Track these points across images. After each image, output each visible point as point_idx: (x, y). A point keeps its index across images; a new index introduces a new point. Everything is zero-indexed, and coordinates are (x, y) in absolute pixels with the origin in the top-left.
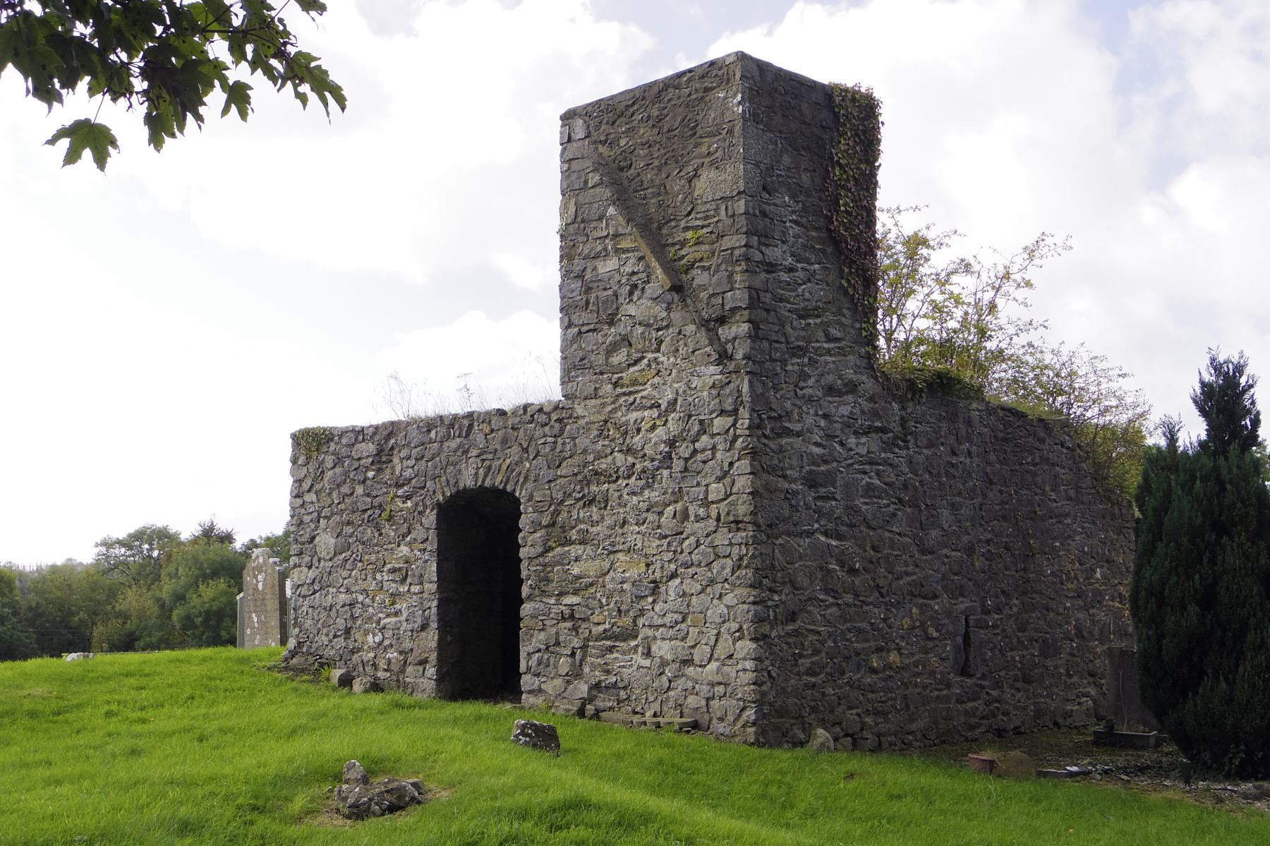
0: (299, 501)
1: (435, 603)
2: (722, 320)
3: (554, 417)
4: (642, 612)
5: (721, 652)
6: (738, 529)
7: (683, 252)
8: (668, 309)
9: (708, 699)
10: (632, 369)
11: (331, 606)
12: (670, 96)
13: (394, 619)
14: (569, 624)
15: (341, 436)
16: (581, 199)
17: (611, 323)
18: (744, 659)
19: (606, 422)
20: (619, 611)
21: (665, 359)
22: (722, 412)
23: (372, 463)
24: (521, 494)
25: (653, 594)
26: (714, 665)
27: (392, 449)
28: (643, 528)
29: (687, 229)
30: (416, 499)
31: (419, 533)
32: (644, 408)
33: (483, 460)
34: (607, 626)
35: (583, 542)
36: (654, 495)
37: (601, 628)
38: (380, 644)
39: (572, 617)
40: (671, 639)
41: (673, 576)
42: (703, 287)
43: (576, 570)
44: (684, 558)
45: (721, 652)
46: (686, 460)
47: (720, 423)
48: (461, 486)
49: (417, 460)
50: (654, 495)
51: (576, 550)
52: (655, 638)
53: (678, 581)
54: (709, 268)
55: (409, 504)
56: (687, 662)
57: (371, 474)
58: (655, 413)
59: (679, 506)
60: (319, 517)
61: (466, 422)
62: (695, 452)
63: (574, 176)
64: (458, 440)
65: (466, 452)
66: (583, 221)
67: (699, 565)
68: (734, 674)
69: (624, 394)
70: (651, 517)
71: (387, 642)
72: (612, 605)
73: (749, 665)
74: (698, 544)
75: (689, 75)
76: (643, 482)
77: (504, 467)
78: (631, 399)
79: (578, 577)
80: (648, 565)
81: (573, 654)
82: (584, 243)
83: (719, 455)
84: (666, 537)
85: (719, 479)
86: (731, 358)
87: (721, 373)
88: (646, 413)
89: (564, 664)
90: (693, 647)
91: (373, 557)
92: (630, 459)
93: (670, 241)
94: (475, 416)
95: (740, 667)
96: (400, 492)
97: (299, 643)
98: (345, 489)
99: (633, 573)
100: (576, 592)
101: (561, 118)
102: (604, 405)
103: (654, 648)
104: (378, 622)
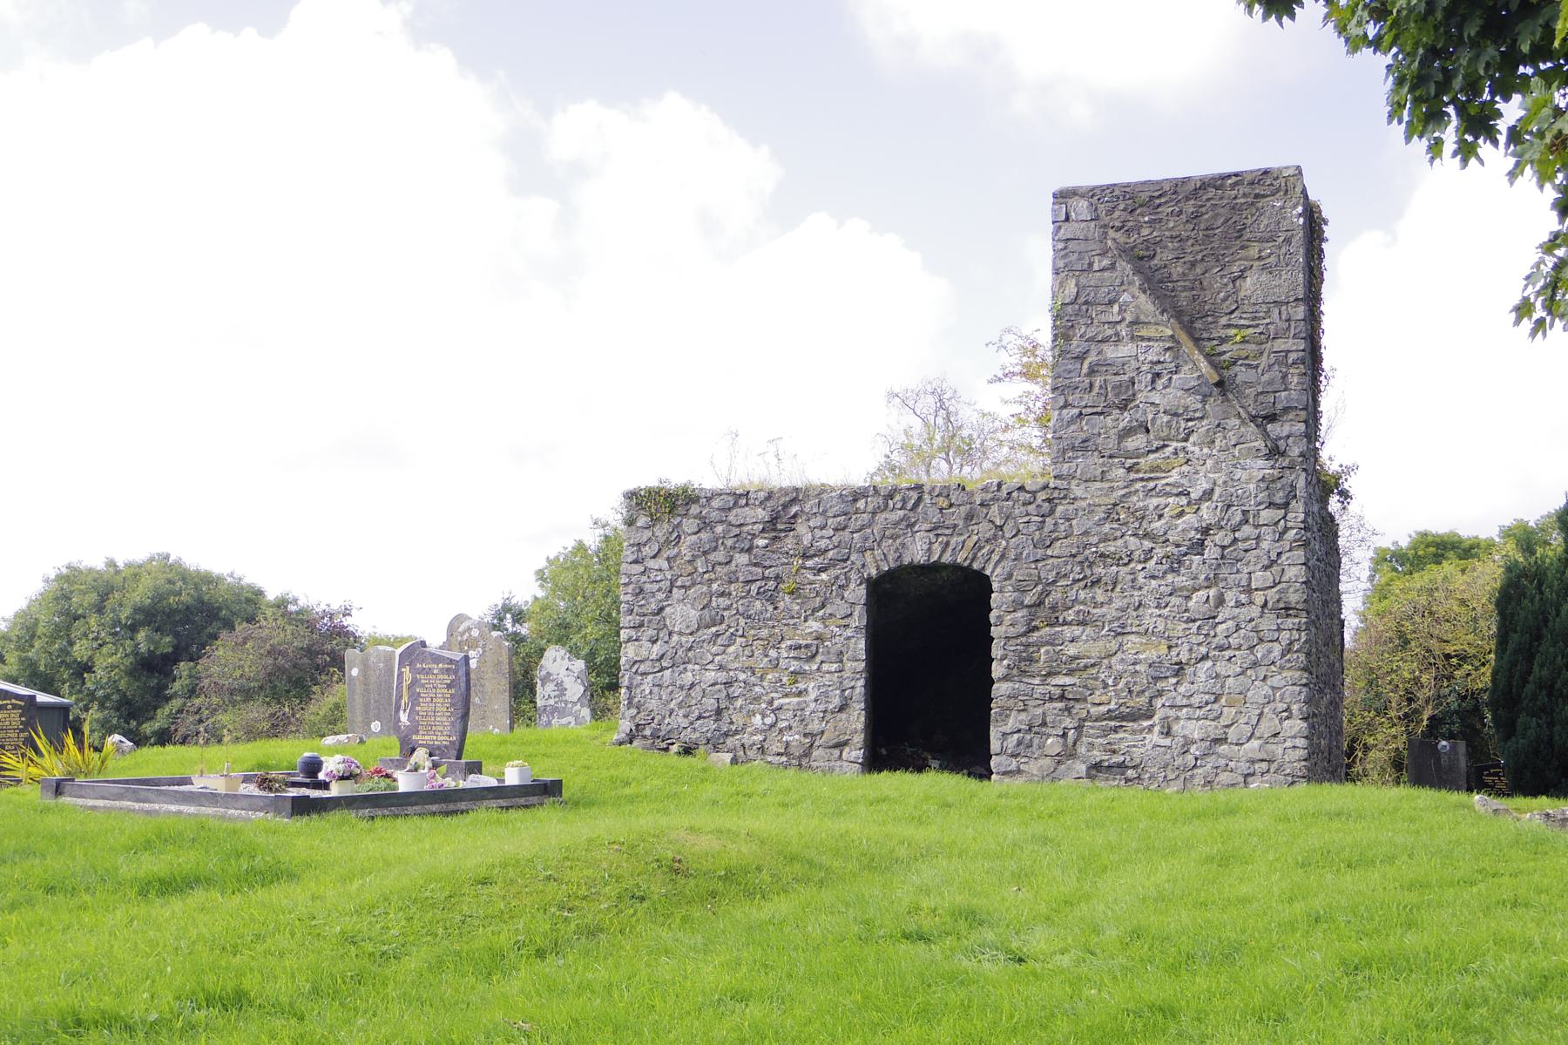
0: (639, 568)
1: (862, 682)
2: (1272, 418)
3: (1041, 496)
4: (1160, 693)
5: (1265, 728)
6: (1288, 616)
7: (1224, 348)
8: (1204, 401)
9: (1246, 776)
10: (1152, 456)
11: (692, 685)
12: (1210, 195)
13: (797, 700)
14: (1060, 705)
15: (709, 499)
16: (1083, 281)
17: (1123, 407)
18: (1294, 737)
19: (1115, 505)
20: (1130, 692)
21: (1197, 449)
22: (1271, 505)
24: (996, 574)
25: (1176, 675)
26: (1255, 743)
28: (1165, 612)
29: (1229, 326)
30: (834, 572)
32: (1168, 494)
33: (938, 535)
34: (1112, 706)
35: (1082, 623)
36: (1181, 580)
37: (1103, 709)
38: (772, 726)
39: (1062, 697)
40: (1198, 719)
41: (1205, 658)
42: (1249, 384)
43: (1072, 650)
45: (1265, 728)
46: (1223, 547)
47: (1267, 515)
48: (906, 561)
49: (836, 530)
50: (1181, 580)
51: (1068, 632)
52: (1178, 718)
53: (1209, 664)
54: (1257, 367)
55: (824, 576)
57: (761, 542)
58: (1184, 501)
59: (1212, 592)
60: (672, 586)
61: (914, 495)
62: (1235, 540)
63: (1074, 257)
64: (901, 513)
65: (912, 525)
66: (1086, 303)
67: (1239, 649)
68: (1280, 751)
69: (1142, 479)
70: (1174, 600)
71: (783, 724)
72: (1121, 685)
73: (1301, 742)
74: (1238, 628)
75: (1234, 179)
76: (1165, 567)
77: (970, 543)
78: (1151, 484)
80: (1170, 647)
81: (1064, 735)
82: (1088, 325)
83: (1265, 545)
84: (1194, 621)
85: (1266, 568)
86: (1283, 454)
87: (1272, 467)
88: (1171, 500)
89: (1053, 744)
90: (1228, 726)
91: (765, 633)
92: (1147, 544)
93: (1205, 335)
94: (926, 489)
95: (1289, 744)
96: (809, 563)
97: (638, 726)
98: (719, 556)
99: (1151, 654)
100: (1070, 673)
101: (1055, 196)
102: (1112, 489)
103: (1175, 728)
104: (771, 703)
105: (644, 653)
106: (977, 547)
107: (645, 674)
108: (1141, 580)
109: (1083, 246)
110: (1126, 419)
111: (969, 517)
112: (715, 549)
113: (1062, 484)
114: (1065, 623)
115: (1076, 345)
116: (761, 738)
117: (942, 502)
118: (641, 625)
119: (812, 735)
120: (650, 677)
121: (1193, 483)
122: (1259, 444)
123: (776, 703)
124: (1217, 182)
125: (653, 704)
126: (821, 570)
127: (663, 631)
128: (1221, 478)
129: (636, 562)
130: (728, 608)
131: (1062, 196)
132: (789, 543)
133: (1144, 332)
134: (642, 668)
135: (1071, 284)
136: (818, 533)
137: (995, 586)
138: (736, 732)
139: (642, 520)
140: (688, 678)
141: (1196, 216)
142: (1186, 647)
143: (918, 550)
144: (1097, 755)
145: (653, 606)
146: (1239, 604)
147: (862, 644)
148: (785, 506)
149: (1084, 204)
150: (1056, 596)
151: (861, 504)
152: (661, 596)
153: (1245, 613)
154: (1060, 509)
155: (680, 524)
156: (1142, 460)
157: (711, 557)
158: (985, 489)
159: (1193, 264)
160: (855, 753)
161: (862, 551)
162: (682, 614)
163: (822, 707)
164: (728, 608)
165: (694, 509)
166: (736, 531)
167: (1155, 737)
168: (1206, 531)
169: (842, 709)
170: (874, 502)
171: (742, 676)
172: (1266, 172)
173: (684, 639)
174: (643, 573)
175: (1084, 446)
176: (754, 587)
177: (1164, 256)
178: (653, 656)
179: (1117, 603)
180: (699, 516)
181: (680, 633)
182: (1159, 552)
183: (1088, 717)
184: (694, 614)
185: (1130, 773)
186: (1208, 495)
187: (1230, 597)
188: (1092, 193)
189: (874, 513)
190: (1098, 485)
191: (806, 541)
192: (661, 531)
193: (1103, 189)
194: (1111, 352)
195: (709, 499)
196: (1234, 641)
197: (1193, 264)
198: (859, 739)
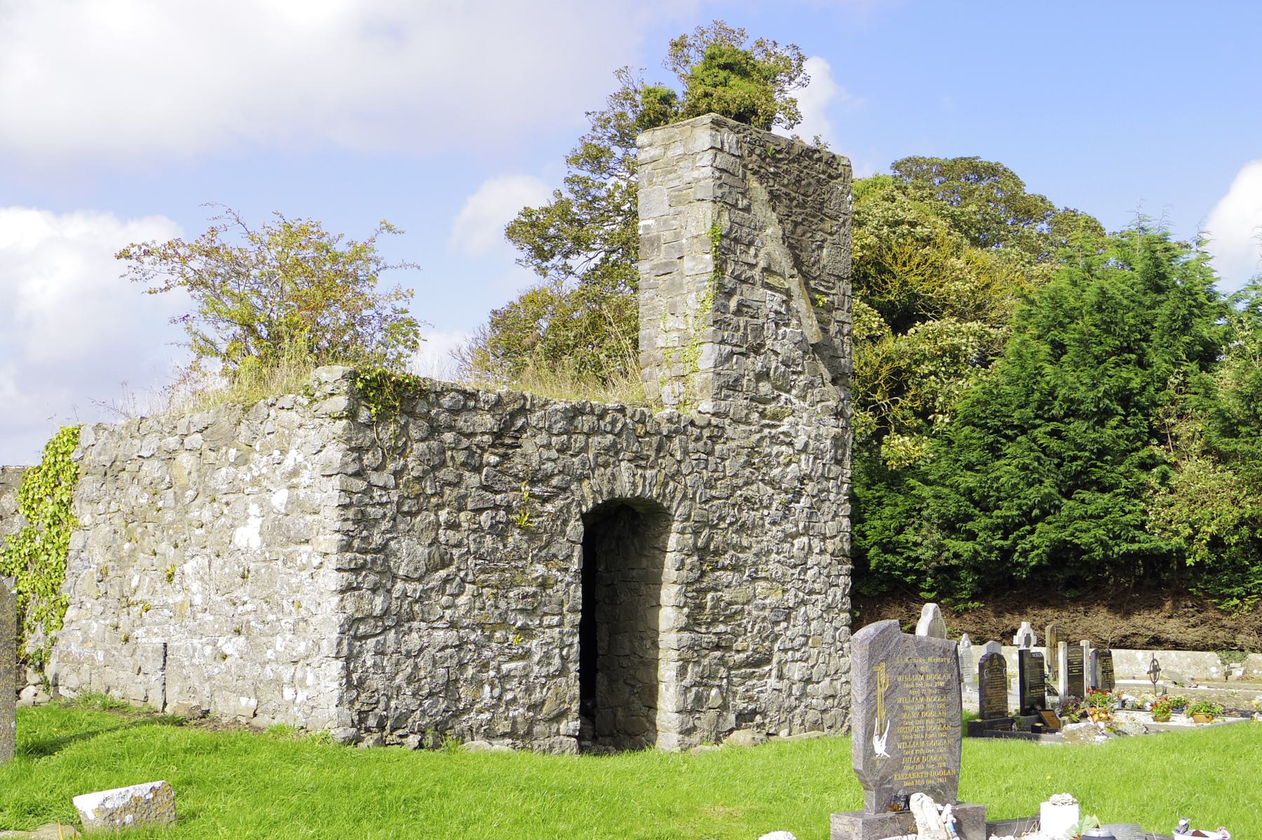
0: (360, 485)
1: (577, 639)
3: (706, 433)
11: (421, 650)
13: (521, 664)
15: (439, 394)
23: (493, 445)
24: (679, 511)
25: (785, 620)
27: (522, 429)
30: (559, 503)
31: (560, 547)
34: (749, 653)
37: (743, 655)
38: (500, 698)
39: (718, 647)
44: (809, 586)
48: (618, 493)
51: (726, 577)
56: (808, 681)
57: (494, 459)
64: (610, 437)
67: (819, 593)
69: (768, 426)
71: (509, 696)
79: (730, 604)
80: (784, 591)
83: (832, 497)
90: (813, 667)
91: (495, 577)
96: (536, 490)
98: (447, 474)
104: (498, 669)
107: (366, 637)
108: (767, 526)
109: (730, 180)
112: (443, 464)
114: (724, 568)
116: (487, 716)
117: (640, 430)
118: (363, 567)
120: (371, 643)
123: (505, 667)
126: (545, 500)
130: (459, 545)
132: (517, 464)
133: (771, 280)
134: (362, 629)
136: (546, 454)
137: (676, 526)
138: (466, 711)
139: (364, 416)
140: (413, 641)
142: (793, 592)
145: (377, 540)
147: (579, 594)
148: (514, 415)
152: (385, 525)
154: (718, 447)
155: (406, 425)
156: (768, 407)
157: (441, 474)
158: (670, 420)
160: (572, 724)
161: (580, 479)
162: (410, 551)
163: (544, 670)
164: (459, 545)
167: (772, 682)
168: (801, 480)
171: (472, 637)
173: (410, 587)
174: (364, 492)
175: (734, 386)
178: (377, 611)
184: (422, 551)
185: (758, 718)
186: (804, 450)
190: (742, 427)
192: (387, 433)
195: (439, 394)
196: (817, 586)
198: (575, 706)
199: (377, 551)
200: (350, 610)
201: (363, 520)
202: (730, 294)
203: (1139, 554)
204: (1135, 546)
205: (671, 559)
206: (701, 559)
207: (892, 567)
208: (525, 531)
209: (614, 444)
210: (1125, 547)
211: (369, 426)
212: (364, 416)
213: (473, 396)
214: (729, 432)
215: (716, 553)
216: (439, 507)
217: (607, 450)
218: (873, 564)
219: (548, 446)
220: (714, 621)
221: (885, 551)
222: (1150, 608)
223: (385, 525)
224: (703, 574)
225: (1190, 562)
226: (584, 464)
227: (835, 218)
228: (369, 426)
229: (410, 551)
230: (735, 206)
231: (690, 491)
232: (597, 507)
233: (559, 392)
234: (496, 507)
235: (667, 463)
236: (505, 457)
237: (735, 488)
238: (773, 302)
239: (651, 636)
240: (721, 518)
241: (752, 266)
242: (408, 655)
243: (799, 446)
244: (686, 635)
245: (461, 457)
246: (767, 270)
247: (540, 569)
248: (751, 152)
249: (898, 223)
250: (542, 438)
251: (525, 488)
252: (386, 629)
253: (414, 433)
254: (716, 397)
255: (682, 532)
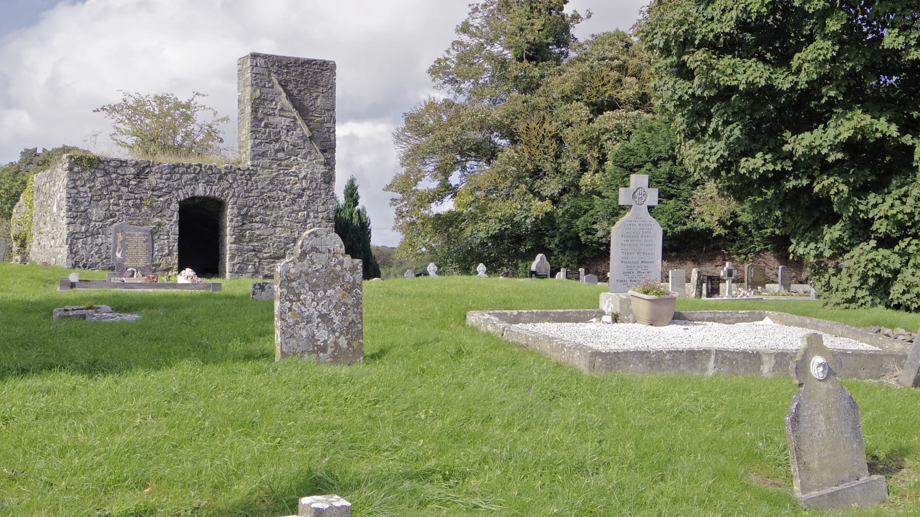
0: (75, 191)
3: (247, 173)
4: (288, 249)
17: (276, 141)
22: (325, 182)
35: (262, 222)
36: (296, 208)
39: (254, 250)
43: (258, 232)
48: (196, 194)
50: (296, 208)
51: (256, 225)
55: (161, 199)
57: (134, 183)
61: (199, 168)
65: (197, 180)
70: (294, 215)
77: (220, 189)
79: (259, 235)
92: (284, 194)
99: (285, 235)
105: (78, 229)
106: (223, 191)
109: (262, 77)
110: (277, 146)
111: (220, 179)
112: (112, 184)
113: (254, 168)
115: (260, 115)
117: (209, 172)
118: (77, 216)
119: (156, 265)
121: (300, 172)
122: (322, 160)
124: (309, 62)
125: (82, 252)
126: (159, 197)
127: (87, 220)
128: (310, 171)
129: (73, 188)
130: (119, 211)
131: (254, 56)
132: (146, 184)
135: (258, 93)
136: (159, 181)
137: (230, 206)
139: (76, 169)
140: (99, 241)
141: (302, 73)
143: (200, 190)
144: (266, 272)
145: (82, 208)
146: (315, 217)
148: (144, 168)
149: (262, 61)
150: (253, 211)
151: (176, 170)
152: (86, 204)
153: (316, 221)
157: (111, 188)
158: (226, 168)
159: (300, 91)
161: (177, 189)
162: (96, 213)
164: (119, 211)
165: (101, 166)
166: (121, 177)
168: (304, 190)
169: (169, 255)
170: (182, 170)
172: (325, 62)
175: (263, 155)
176: (130, 203)
177: (291, 86)
179: (274, 215)
180: (104, 169)
181: (96, 221)
182: (288, 197)
183: (263, 258)
184: (102, 213)
186: (305, 177)
187: (312, 215)
188: (265, 57)
189: (182, 174)
191: (154, 183)
192: (86, 175)
193: (270, 56)
194: (271, 119)
195: (109, 162)
197: (300, 91)
199: (83, 212)
200: (71, 229)
201: (75, 202)
202: (261, 120)
203: (690, 231)
204: (685, 228)
205: (228, 218)
206: (243, 219)
207: (592, 242)
208: (149, 207)
209: (195, 177)
210: (680, 228)
211: (79, 173)
212: (76, 169)
213: (126, 162)
214: (260, 172)
215: (251, 216)
216: (109, 199)
217: (191, 179)
218: (583, 239)
219: (161, 178)
220: (250, 241)
221: (588, 234)
222: (710, 261)
223: (86, 204)
224: (244, 224)
225: (714, 235)
226: (179, 185)
227: (326, 86)
228: (79, 173)
229: (96, 213)
230: (264, 86)
231: (237, 194)
232: (185, 200)
233: (167, 160)
234: (135, 199)
235: (225, 184)
236: (140, 182)
237: (262, 193)
238: (285, 122)
239: (224, 245)
240: (254, 204)
241: (273, 109)
242: (96, 245)
243: (301, 176)
244: (234, 245)
245: (119, 182)
246: (282, 110)
247: (157, 220)
248: (272, 66)
249: (603, 59)
250: (159, 175)
251: (150, 193)
252: (86, 237)
253: (98, 175)
254: (252, 159)
255: (232, 208)
